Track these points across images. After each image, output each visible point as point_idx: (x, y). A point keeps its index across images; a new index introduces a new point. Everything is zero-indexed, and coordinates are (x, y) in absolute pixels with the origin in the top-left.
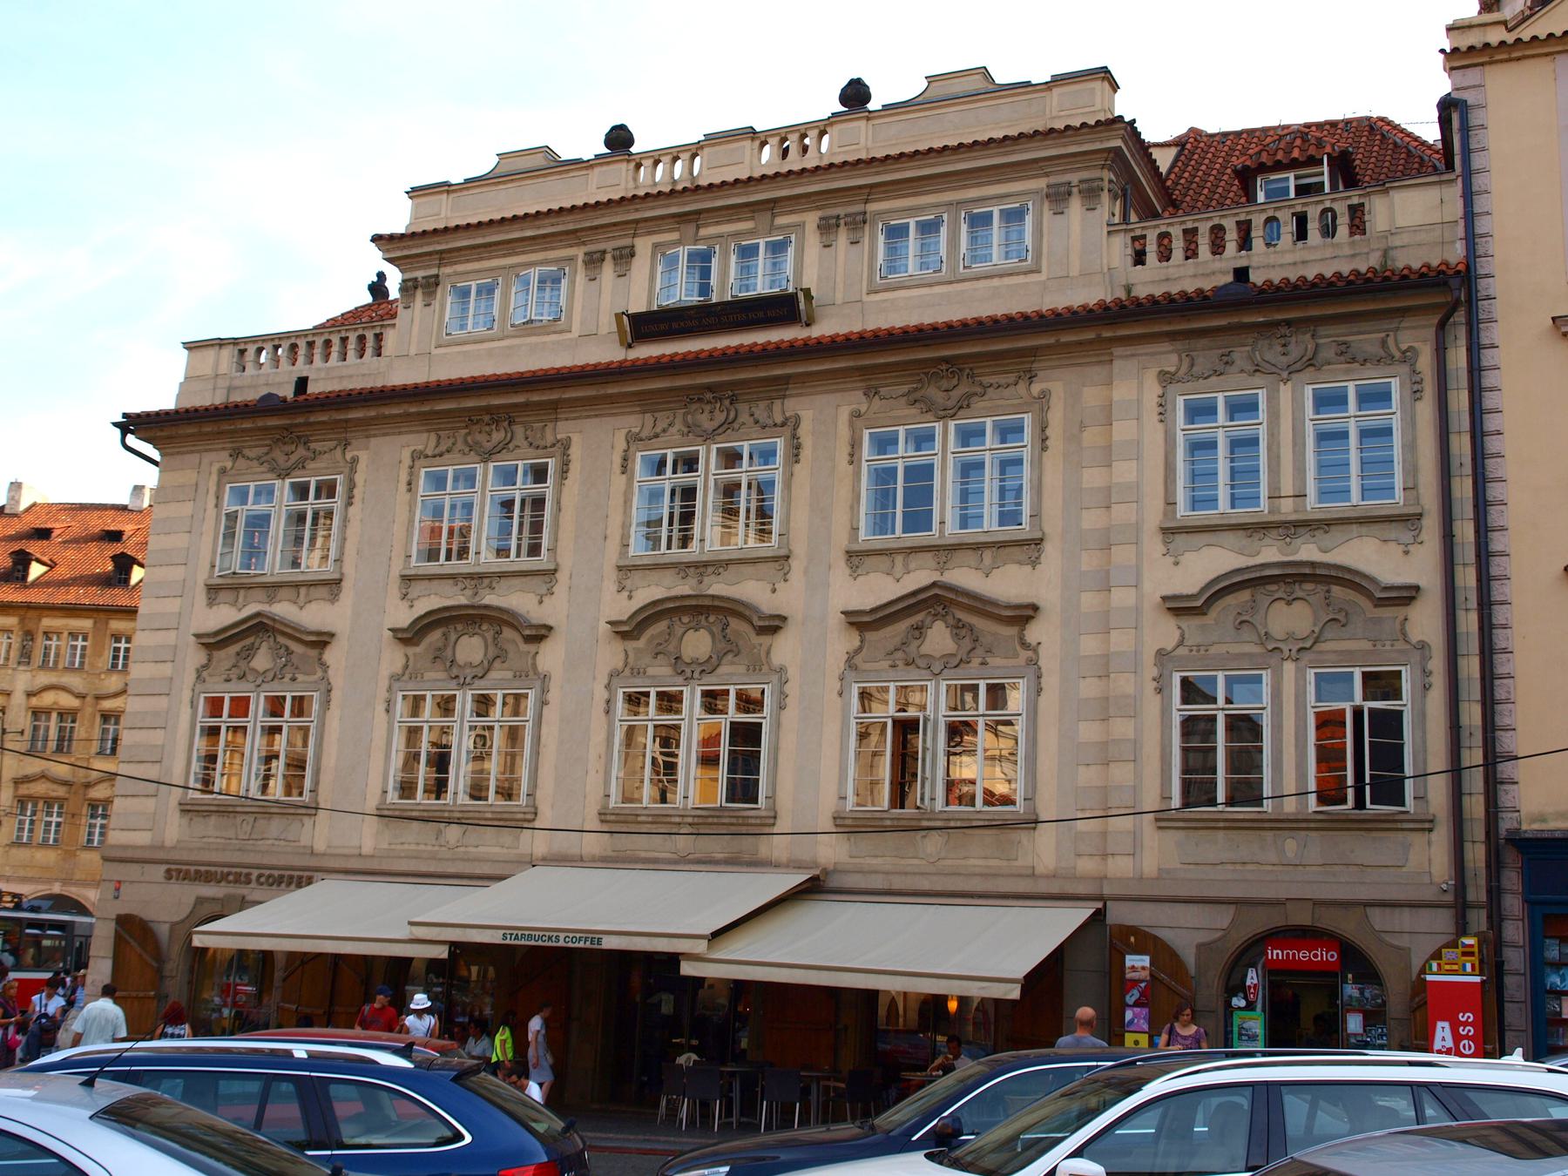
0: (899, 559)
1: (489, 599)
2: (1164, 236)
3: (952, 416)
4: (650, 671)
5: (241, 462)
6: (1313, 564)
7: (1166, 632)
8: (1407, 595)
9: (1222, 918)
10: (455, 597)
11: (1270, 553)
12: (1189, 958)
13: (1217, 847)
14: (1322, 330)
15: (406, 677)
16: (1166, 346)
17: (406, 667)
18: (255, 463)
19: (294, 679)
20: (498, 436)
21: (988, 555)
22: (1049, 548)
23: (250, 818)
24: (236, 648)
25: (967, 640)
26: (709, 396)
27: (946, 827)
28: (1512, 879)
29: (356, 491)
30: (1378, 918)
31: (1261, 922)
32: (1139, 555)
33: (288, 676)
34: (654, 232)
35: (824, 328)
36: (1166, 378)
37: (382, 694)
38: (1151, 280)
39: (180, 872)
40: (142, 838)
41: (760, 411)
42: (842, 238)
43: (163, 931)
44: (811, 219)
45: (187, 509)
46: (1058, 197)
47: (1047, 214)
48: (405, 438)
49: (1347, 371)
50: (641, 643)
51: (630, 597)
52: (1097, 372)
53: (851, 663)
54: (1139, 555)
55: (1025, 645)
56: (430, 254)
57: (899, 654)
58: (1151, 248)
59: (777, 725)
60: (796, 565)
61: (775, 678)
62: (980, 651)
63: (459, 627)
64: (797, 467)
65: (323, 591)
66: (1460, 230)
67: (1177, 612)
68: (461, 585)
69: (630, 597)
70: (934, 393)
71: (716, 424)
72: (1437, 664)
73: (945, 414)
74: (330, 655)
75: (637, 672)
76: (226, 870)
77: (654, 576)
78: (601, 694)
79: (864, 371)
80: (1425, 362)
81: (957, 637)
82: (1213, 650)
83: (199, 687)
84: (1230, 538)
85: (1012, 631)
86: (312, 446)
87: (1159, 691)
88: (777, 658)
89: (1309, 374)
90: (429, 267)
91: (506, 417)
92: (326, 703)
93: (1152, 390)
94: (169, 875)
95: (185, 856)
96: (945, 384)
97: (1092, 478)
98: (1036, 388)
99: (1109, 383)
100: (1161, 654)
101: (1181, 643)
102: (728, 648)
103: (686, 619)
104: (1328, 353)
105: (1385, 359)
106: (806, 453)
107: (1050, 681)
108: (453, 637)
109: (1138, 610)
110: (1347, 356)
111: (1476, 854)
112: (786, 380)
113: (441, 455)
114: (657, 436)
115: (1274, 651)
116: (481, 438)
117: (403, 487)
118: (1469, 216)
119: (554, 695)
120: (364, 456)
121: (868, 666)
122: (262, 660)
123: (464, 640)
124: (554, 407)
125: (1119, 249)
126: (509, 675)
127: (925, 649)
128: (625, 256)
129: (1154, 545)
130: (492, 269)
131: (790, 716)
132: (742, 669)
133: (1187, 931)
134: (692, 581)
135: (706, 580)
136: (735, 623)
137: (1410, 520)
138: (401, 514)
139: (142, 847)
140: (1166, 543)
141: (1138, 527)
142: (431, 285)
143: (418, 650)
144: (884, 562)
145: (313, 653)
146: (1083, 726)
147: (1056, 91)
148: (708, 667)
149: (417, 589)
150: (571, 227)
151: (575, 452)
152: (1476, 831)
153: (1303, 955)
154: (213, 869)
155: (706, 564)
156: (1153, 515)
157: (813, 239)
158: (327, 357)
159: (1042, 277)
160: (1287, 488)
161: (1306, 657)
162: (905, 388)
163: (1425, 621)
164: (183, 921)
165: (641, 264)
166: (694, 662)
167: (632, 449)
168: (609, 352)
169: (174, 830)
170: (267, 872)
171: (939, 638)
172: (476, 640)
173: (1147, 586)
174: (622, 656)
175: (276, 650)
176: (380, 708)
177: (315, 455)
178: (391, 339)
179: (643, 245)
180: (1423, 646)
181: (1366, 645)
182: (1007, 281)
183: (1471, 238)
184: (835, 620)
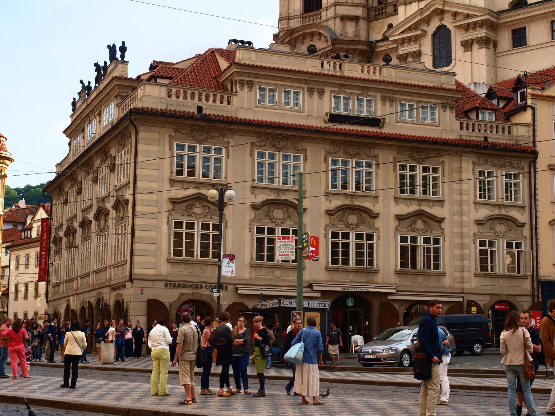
0: (408, 201)
1: (283, 198)
2: (468, 124)
3: (421, 164)
4: (338, 226)
5: (178, 134)
6: (507, 216)
7: (475, 229)
8: (523, 225)
9: (488, 298)
10: (272, 196)
11: (496, 212)
12: (482, 306)
13: (487, 282)
14: (507, 158)
15: (256, 220)
16: (474, 155)
17: (255, 217)
18: (186, 136)
19: (211, 218)
20: (282, 144)
21: (431, 203)
22: (446, 204)
23: (199, 266)
24: (187, 204)
25: (427, 226)
26: (353, 144)
27: (424, 275)
28: (540, 290)
29: (230, 153)
30: (518, 299)
31: (497, 299)
32: (469, 208)
33: (209, 217)
34: (331, 87)
35: (386, 130)
36: (474, 164)
37: (247, 226)
38: (466, 135)
39: (169, 284)
40: (151, 272)
41: (367, 151)
42: (388, 104)
43: (167, 305)
44: (379, 96)
45: (156, 148)
46: (444, 107)
47: (441, 111)
48: (250, 138)
49: (512, 169)
50: (335, 217)
51: (330, 203)
52: (457, 158)
53: (397, 229)
54: (469, 208)
55: (441, 228)
56: (253, 73)
57: (409, 228)
58: (465, 126)
59: (377, 244)
60: (380, 199)
61: (377, 231)
62: (430, 229)
63: (274, 206)
64: (379, 170)
66: (532, 139)
67: (478, 224)
68: (273, 192)
69: (330, 203)
71: (354, 153)
72: (528, 241)
75: (334, 226)
76: (191, 284)
77: (338, 197)
79: (399, 146)
80: (526, 170)
81: (424, 224)
82: (485, 234)
83: (170, 218)
84: (488, 207)
85: (437, 224)
86: (210, 134)
87: (474, 243)
88: (376, 225)
89: (503, 169)
90: (250, 77)
91: (286, 138)
92: (226, 227)
93: (471, 166)
94: (166, 285)
95: (169, 279)
96: (419, 154)
97: (456, 186)
98: (441, 159)
99: (461, 162)
100: (474, 234)
101: (478, 232)
103: (348, 211)
104: (507, 164)
105: (518, 168)
107: (447, 238)
108: (272, 209)
109: (469, 223)
110: (511, 165)
111: (535, 284)
113: (262, 146)
114: (335, 153)
115: (497, 236)
116: (276, 143)
118: (534, 136)
121: (401, 230)
122: (198, 210)
123: (276, 210)
124: (302, 138)
125: (457, 125)
126: (292, 223)
127: (416, 227)
128: (321, 93)
129: (472, 206)
130: (274, 84)
131: (381, 242)
132: (366, 228)
133: (482, 301)
134: (350, 200)
135: (354, 200)
136: (364, 215)
137: (523, 207)
138: (248, 165)
139: (153, 275)
140: (475, 206)
141: (468, 201)
143: (259, 212)
144: (404, 201)
146: (455, 250)
147: (443, 76)
148: (357, 226)
149: (257, 191)
150: (307, 78)
151: (309, 153)
152: (535, 280)
153: (502, 307)
154: (186, 283)
155: (354, 195)
156: (472, 199)
158: (221, 102)
159: (440, 128)
160: (500, 197)
161: (504, 238)
162: (408, 153)
163: (526, 232)
164: (175, 301)
165: (327, 96)
166: (352, 224)
167: (328, 156)
168: (319, 123)
169: (165, 269)
170: (209, 285)
172: (280, 211)
173: (471, 217)
174: (329, 220)
176: (247, 230)
177: (212, 138)
178: (235, 100)
179: (327, 90)
180: (525, 237)
181: (515, 236)
182: (432, 127)
183: (534, 142)
184: (392, 217)
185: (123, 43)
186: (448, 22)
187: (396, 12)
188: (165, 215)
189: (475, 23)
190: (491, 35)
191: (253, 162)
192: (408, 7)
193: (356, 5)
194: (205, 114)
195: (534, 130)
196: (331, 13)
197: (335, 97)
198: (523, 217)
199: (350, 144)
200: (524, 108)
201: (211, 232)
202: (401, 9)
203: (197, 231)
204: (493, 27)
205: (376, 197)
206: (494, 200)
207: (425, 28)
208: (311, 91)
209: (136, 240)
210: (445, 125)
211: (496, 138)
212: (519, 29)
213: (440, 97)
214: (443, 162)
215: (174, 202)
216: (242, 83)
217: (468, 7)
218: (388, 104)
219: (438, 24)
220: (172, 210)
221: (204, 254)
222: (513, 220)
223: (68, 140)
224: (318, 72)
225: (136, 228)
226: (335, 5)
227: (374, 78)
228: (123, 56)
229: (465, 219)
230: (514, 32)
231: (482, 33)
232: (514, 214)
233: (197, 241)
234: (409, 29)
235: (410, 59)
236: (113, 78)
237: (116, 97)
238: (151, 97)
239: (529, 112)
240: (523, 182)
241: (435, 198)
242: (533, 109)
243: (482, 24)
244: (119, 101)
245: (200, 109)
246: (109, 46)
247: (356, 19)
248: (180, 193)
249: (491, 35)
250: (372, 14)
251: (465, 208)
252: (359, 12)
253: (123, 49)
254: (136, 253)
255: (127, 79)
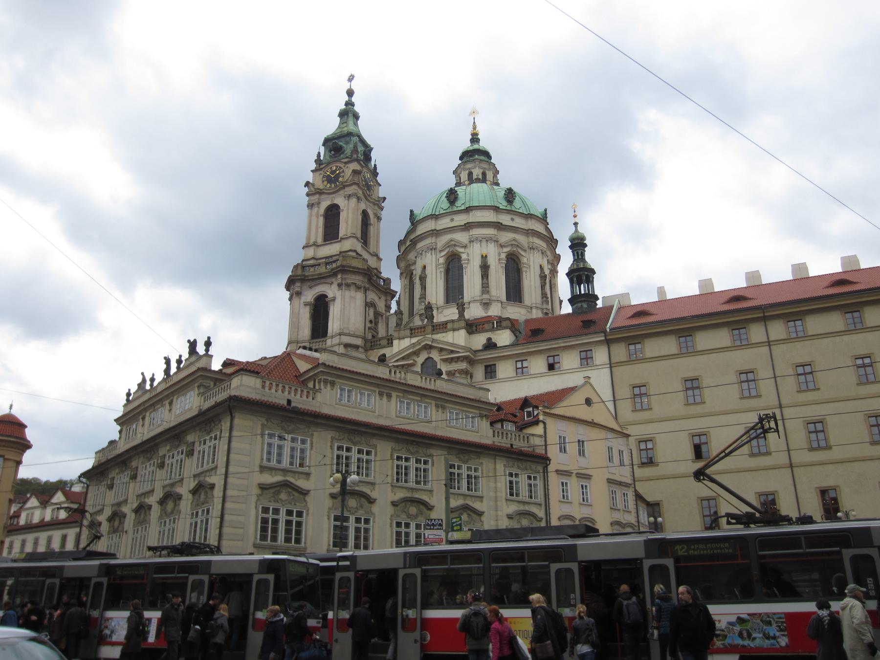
1: (357, 488)
20: (357, 439)
36: (505, 466)
46: (481, 416)
60: (435, 493)
65: (304, 476)
70: (461, 456)
73: (465, 462)
74: (307, 498)
75: (398, 516)
78: (389, 521)
79: (449, 448)
91: (360, 433)
92: (308, 514)
93: (503, 468)
102: (421, 513)
106: (435, 464)
112: (432, 445)
117: (329, 447)
119: (376, 520)
120: (315, 433)
122: (283, 496)
124: (374, 435)
128: (389, 396)
137: (540, 505)
142: (333, 384)
145: (302, 496)
148: (416, 517)
157: (434, 408)
171: (464, 517)
172: (354, 500)
175: (289, 494)
176: (326, 518)
178: (319, 396)
179: (394, 394)
185: (209, 338)
186: (435, 356)
187: (390, 343)
188: (254, 498)
189: (458, 358)
190: (469, 368)
191: (332, 453)
192: (402, 341)
193: (357, 337)
194: (296, 407)
195: (546, 441)
196: (336, 340)
197: (401, 402)
198: (541, 513)
199: (412, 443)
200: (536, 422)
201: (294, 519)
202: (395, 342)
203: (282, 517)
204: (471, 362)
205: (431, 491)
206: (520, 498)
207: (415, 358)
208: (381, 394)
209: (225, 523)
210: (481, 432)
211: (519, 444)
212: (490, 366)
213: (479, 408)
214: (482, 463)
215: (263, 487)
216: (326, 382)
217: (452, 345)
218: (440, 410)
219: (427, 356)
220: (261, 495)
221: (288, 540)
222: (534, 515)
223: (119, 428)
224: (385, 377)
225: (226, 511)
226: (340, 334)
227: (429, 387)
228: (207, 350)
229: (500, 513)
230: (486, 367)
231: (463, 365)
232: (534, 509)
233: (282, 527)
234: (403, 358)
235: (457, 375)
236: (199, 369)
237: (199, 387)
238: (245, 387)
239: (541, 425)
240: (539, 483)
241: (477, 494)
242: (544, 423)
243: (465, 358)
244: (202, 390)
245: (289, 402)
246: (189, 341)
247: (356, 347)
248: (268, 479)
249: (469, 368)
250: (369, 344)
251: (499, 503)
252: (359, 342)
253: (208, 344)
254: (225, 537)
255: (211, 371)
